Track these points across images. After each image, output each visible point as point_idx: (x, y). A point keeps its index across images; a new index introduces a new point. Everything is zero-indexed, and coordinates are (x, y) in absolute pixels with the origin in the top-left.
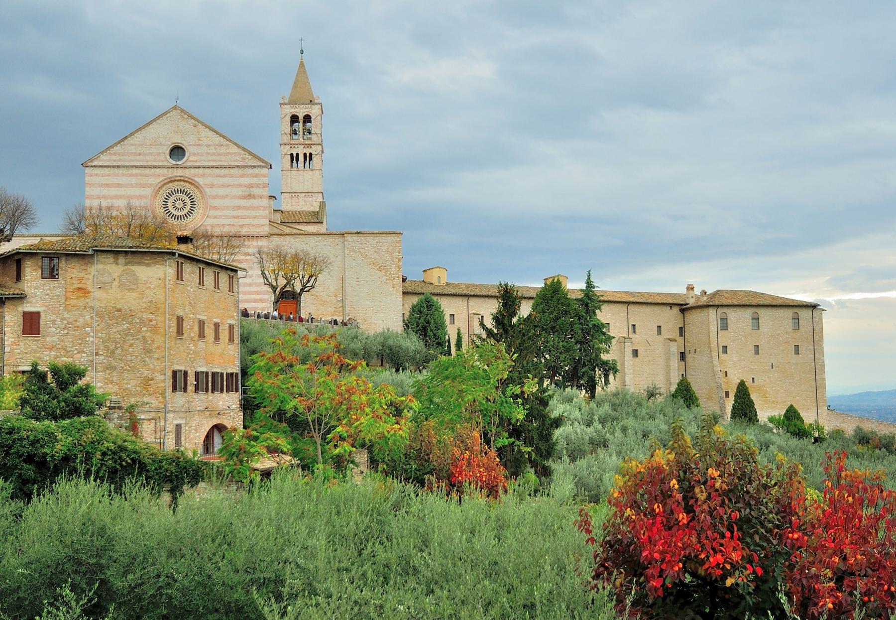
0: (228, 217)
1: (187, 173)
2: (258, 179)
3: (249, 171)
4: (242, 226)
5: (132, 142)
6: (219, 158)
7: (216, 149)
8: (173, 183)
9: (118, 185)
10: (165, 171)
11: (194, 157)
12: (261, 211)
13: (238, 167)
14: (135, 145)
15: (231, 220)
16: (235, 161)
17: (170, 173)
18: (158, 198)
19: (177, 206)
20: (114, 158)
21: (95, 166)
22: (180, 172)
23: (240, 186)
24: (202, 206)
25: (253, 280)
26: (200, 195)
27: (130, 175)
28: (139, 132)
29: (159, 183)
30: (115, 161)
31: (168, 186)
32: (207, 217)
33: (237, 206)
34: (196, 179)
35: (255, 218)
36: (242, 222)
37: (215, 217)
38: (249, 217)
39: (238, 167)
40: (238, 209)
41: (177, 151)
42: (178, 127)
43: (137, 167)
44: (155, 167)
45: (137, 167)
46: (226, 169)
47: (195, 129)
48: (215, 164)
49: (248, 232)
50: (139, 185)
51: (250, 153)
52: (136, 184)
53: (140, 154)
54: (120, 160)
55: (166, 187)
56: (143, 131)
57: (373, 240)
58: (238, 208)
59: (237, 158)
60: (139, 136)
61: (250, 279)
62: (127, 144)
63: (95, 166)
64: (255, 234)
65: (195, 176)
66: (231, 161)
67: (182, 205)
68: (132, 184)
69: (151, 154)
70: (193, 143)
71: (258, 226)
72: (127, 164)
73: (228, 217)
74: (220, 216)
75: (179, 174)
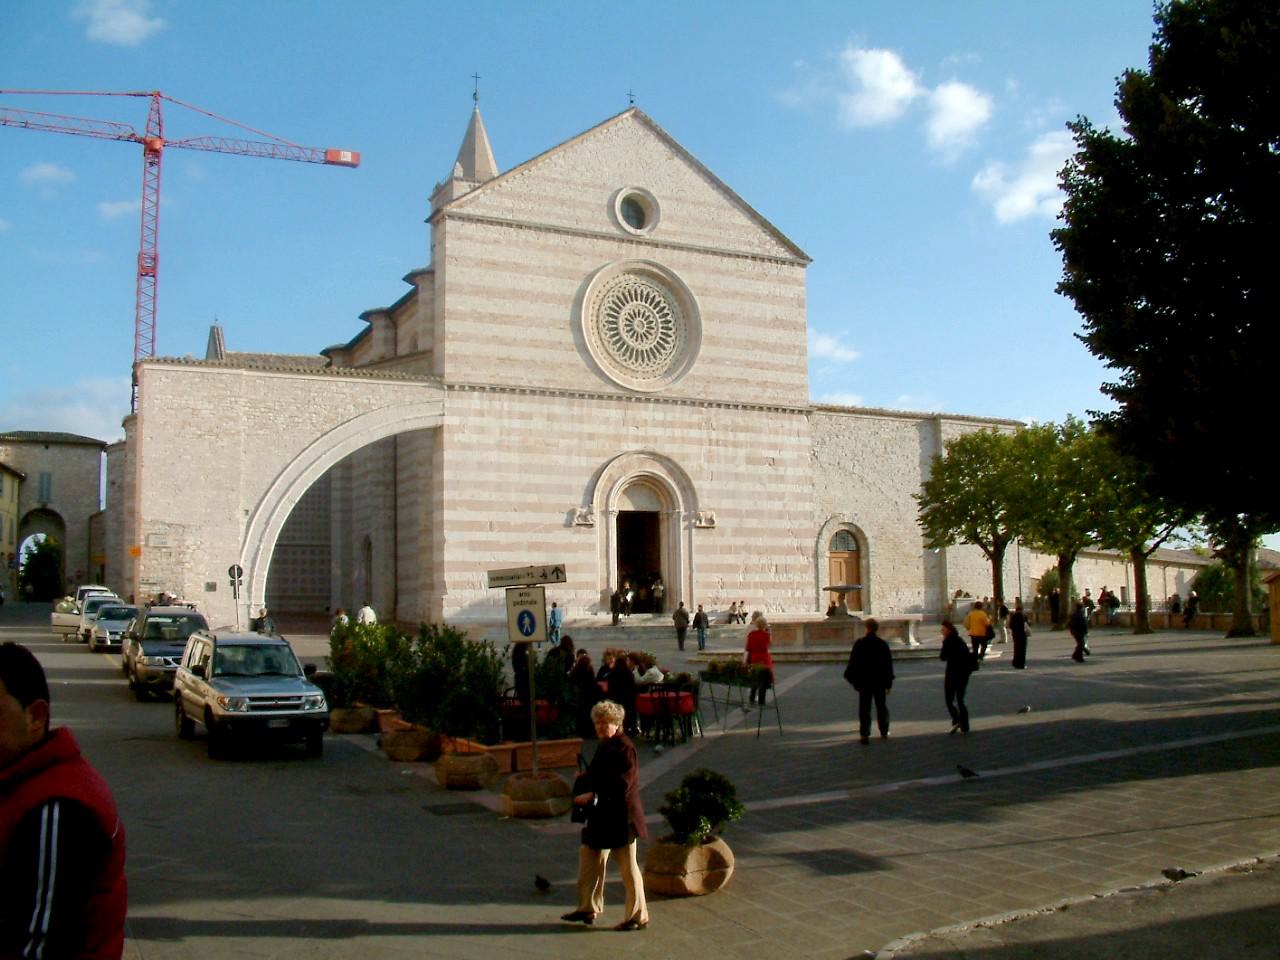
1: (660, 257)
3: (772, 269)
4: (764, 384)
9: (517, 267)
10: (612, 246)
13: (754, 258)
14: (554, 180)
15: (742, 370)
19: (636, 328)
20: (508, 203)
21: (470, 219)
22: (644, 253)
23: (757, 297)
25: (785, 505)
27: (544, 248)
28: (561, 154)
33: (751, 342)
34: (676, 272)
35: (783, 369)
37: (713, 361)
38: (774, 367)
39: (754, 258)
43: (557, 231)
44: (595, 236)
45: (557, 231)
48: (710, 245)
49: (774, 398)
51: (765, 225)
53: (563, 203)
54: (521, 211)
58: (755, 345)
60: (561, 161)
61: (780, 503)
62: (537, 176)
63: (470, 219)
68: (545, 267)
72: (536, 220)
75: (641, 257)
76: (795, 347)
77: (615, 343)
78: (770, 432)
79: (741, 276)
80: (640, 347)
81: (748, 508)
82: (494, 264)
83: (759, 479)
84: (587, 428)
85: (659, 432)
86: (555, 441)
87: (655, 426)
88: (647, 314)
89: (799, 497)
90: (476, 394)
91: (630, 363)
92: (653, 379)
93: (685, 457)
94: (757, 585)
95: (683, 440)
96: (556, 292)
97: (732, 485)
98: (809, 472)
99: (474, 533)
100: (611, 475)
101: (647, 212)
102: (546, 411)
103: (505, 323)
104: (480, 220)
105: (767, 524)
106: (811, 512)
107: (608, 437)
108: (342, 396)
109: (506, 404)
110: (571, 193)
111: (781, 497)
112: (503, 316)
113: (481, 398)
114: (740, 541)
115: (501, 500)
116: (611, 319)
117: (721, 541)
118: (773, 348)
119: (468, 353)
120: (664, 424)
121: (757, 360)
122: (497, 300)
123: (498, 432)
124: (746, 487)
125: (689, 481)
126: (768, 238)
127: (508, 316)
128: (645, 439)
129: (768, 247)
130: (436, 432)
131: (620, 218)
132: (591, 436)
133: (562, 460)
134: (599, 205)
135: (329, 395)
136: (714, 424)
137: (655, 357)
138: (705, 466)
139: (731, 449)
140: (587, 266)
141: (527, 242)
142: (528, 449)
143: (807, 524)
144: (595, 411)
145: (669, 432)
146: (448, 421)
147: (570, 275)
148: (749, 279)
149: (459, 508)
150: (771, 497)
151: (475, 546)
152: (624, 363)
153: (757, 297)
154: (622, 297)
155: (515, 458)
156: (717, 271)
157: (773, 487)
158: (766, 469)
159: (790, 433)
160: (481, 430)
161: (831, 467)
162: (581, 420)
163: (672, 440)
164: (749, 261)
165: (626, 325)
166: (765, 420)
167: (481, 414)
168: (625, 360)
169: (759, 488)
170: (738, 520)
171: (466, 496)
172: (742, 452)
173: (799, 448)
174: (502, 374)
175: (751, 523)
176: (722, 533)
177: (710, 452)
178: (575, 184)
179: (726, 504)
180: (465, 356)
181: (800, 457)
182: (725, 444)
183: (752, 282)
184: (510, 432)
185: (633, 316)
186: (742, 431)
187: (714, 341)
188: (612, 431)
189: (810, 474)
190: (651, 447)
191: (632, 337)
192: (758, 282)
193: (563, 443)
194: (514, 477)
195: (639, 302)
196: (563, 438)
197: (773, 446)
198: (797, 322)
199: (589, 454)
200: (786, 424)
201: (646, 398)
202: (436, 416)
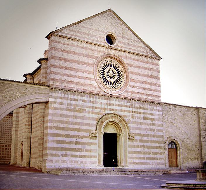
2: (155, 66)
3: (150, 60)
4: (148, 95)
6: (134, 48)
8: (107, 59)
11: (120, 45)
12: (158, 87)
14: (86, 28)
17: (107, 51)
18: (98, 67)
19: (110, 75)
20: (72, 33)
22: (112, 52)
23: (146, 68)
24: (124, 78)
25: (155, 133)
26: (123, 70)
29: (101, 56)
31: (104, 60)
32: (129, 86)
35: (154, 91)
38: (151, 90)
40: (145, 84)
47: (121, 26)
52: (86, 55)
53: (88, 35)
55: (103, 61)
56: (91, 20)
58: (145, 83)
59: (143, 50)
60: (88, 22)
68: (83, 54)
69: (95, 36)
74: (135, 86)
76: (157, 84)
77: (104, 79)
78: (150, 110)
79: (141, 62)
80: (111, 81)
81: (144, 133)
83: (147, 124)
84: (95, 105)
85: (117, 108)
86: (84, 109)
87: (116, 106)
88: (113, 71)
89: (159, 131)
90: (60, 92)
91: (108, 85)
92: (115, 91)
93: (125, 116)
94: (147, 158)
95: (124, 111)
96: (86, 62)
97: (139, 126)
98: (161, 123)
99: (57, 137)
100: (102, 121)
101: (113, 41)
102: (82, 99)
103: (70, 70)
104: (63, 37)
105: (150, 139)
106: (163, 136)
107: (101, 108)
108: (16, 89)
109: (69, 96)
110: (91, 32)
111: (154, 130)
112: (69, 67)
113: (61, 93)
114: (142, 144)
115: (67, 127)
116: (102, 72)
117: (136, 144)
118: (150, 84)
119: (58, 78)
120: (119, 105)
121: (146, 87)
122: (67, 62)
123: (67, 104)
124: (143, 126)
125: (126, 123)
126: (149, 51)
127: (71, 68)
128: (113, 110)
129: (149, 54)
130: (47, 103)
131: (106, 41)
132: (96, 108)
133: (87, 115)
134: (99, 37)
135: (11, 88)
136: (134, 106)
137: (116, 84)
138: (131, 119)
139: (139, 114)
140: (96, 54)
141: (77, 46)
142: (77, 111)
143: (162, 139)
144: (98, 100)
145: (120, 108)
146: (51, 100)
148: (144, 63)
149: (53, 129)
150: (151, 130)
151: (58, 142)
152: (107, 86)
153: (146, 68)
154: (106, 65)
155: (72, 113)
156: (134, 60)
157: (151, 127)
158: (150, 122)
159: (156, 110)
160: (61, 104)
161: (168, 122)
162: (93, 102)
163: (121, 111)
165: (107, 74)
166: (149, 106)
167: (61, 98)
168: (107, 85)
169: (147, 127)
170: (141, 137)
171: (56, 125)
172: (142, 116)
173: (159, 115)
174: (68, 86)
175: (145, 138)
176: (136, 141)
177: (133, 115)
178: (92, 29)
179: (138, 132)
180: (56, 79)
181: (159, 118)
182: (137, 113)
183: (144, 64)
184: (71, 105)
186: (142, 109)
187: (133, 80)
188: (103, 106)
189: (162, 124)
190: (115, 112)
191: (109, 78)
192: (146, 64)
193: (87, 109)
194: (71, 120)
195: (111, 67)
196: (87, 108)
197: (151, 114)
198: (158, 77)
199: (95, 113)
200: (155, 108)
201: (113, 96)
202: (47, 98)
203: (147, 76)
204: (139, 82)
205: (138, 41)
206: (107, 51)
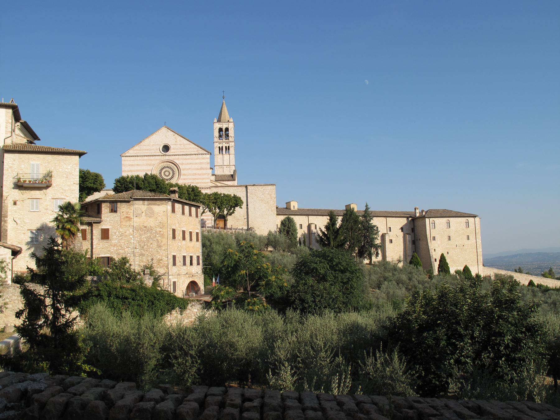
0: (190, 179)
1: (171, 158)
5: (144, 144)
6: (186, 150)
7: (184, 146)
9: (138, 165)
10: (160, 157)
16: (193, 152)
17: (162, 158)
20: (135, 152)
22: (167, 158)
23: (196, 164)
27: (143, 160)
30: (136, 153)
34: (175, 161)
35: (203, 179)
36: (197, 181)
38: (200, 179)
41: (166, 148)
42: (166, 136)
46: (189, 156)
50: (147, 165)
53: (148, 150)
55: (160, 165)
57: (262, 188)
58: (196, 174)
59: (194, 150)
64: (204, 187)
65: (174, 159)
66: (192, 152)
67: (168, 174)
70: (173, 143)
71: (205, 183)
72: (142, 154)
73: (190, 179)
79: (192, 159)
82: (132, 165)
110: (150, 147)
140: (153, 162)
147: (150, 165)
153: (196, 164)
164: (194, 155)
185: (164, 173)
187: (184, 175)
203: (198, 169)
204: (190, 175)
205: (189, 144)
206: (162, 158)
